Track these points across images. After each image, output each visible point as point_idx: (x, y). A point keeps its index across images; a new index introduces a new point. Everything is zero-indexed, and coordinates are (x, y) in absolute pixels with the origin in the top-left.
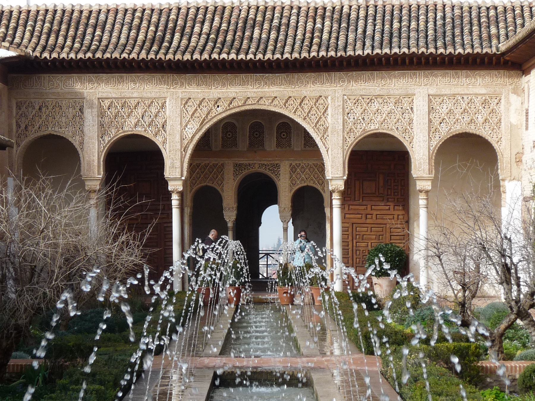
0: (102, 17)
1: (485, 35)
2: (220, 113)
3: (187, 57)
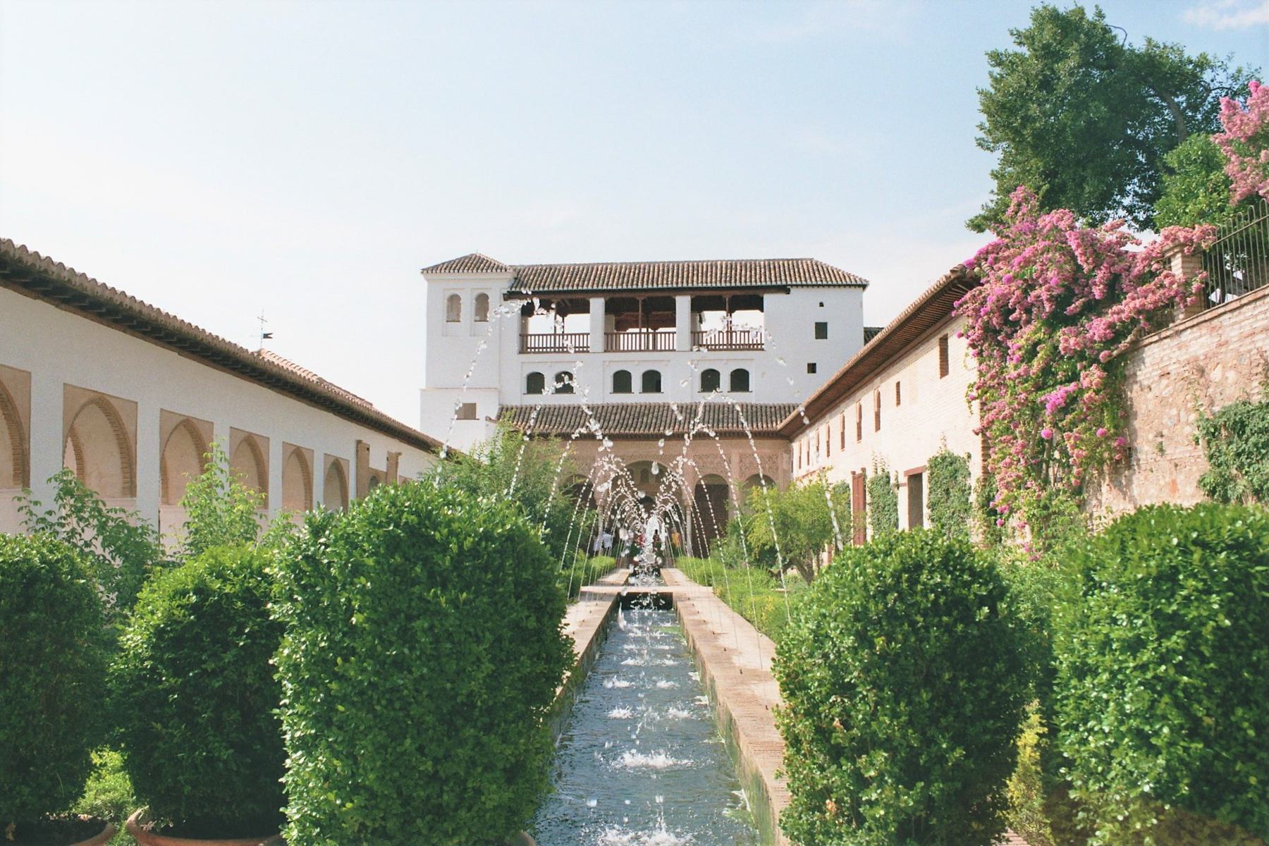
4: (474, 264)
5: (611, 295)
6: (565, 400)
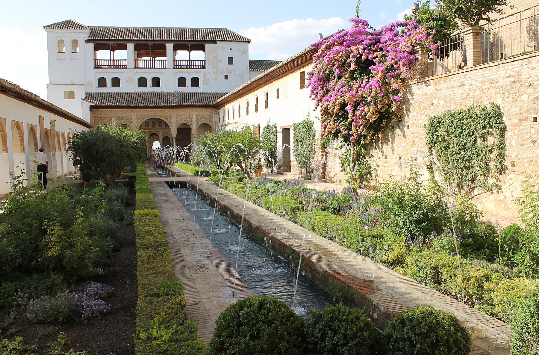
2: (146, 119)
4: (69, 25)
5: (137, 42)
6: (116, 90)
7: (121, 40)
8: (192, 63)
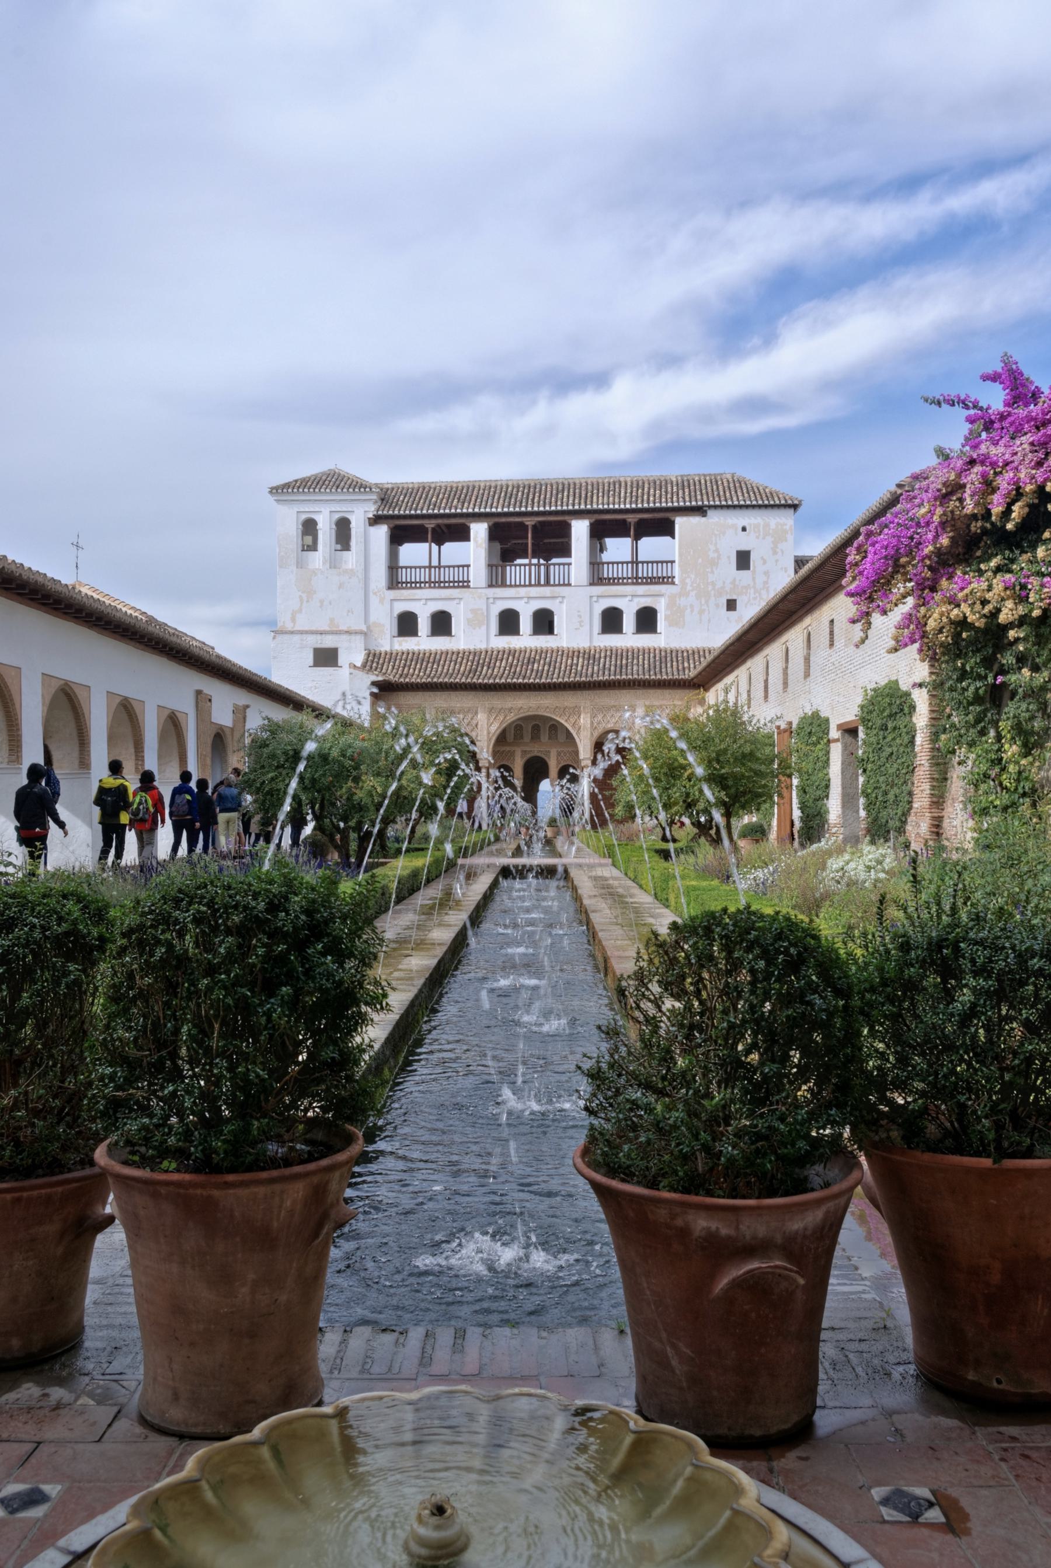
0: (438, 657)
1: (680, 667)
2: (511, 718)
3: (491, 681)
4: (332, 482)
5: (497, 520)
7: (455, 515)
8: (643, 571)
